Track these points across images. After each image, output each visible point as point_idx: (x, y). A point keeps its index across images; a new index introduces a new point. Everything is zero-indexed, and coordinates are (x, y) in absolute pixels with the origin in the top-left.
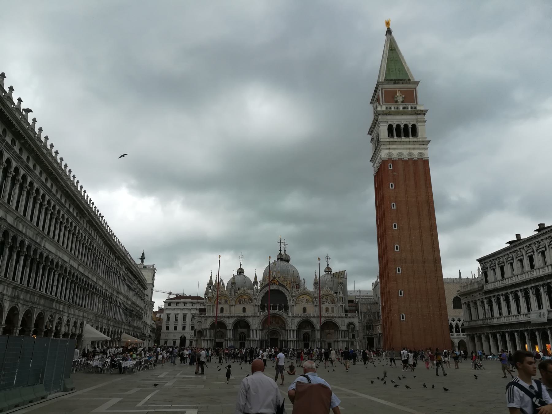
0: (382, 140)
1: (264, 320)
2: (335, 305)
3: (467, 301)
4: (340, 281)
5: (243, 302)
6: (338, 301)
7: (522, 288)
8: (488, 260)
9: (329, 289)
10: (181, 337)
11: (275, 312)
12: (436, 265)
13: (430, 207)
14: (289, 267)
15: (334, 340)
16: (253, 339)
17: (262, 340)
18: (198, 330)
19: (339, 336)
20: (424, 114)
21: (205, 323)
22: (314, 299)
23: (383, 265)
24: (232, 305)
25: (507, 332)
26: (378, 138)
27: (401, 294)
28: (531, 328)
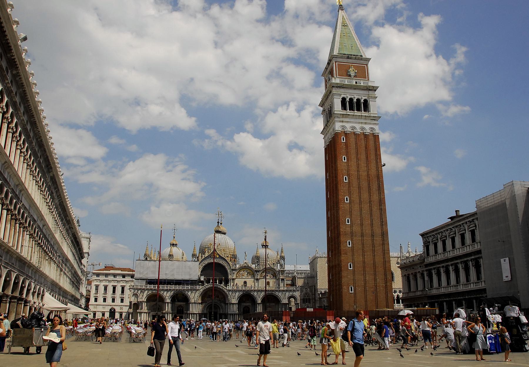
0: (335, 112)
2: (276, 279)
3: (406, 274)
7: (462, 260)
8: (431, 234)
10: (111, 310)
12: (384, 239)
13: (379, 182)
16: (192, 312)
20: (375, 90)
22: (255, 272)
23: (332, 238)
25: (445, 301)
26: (331, 111)
27: (350, 267)
28: (469, 297)
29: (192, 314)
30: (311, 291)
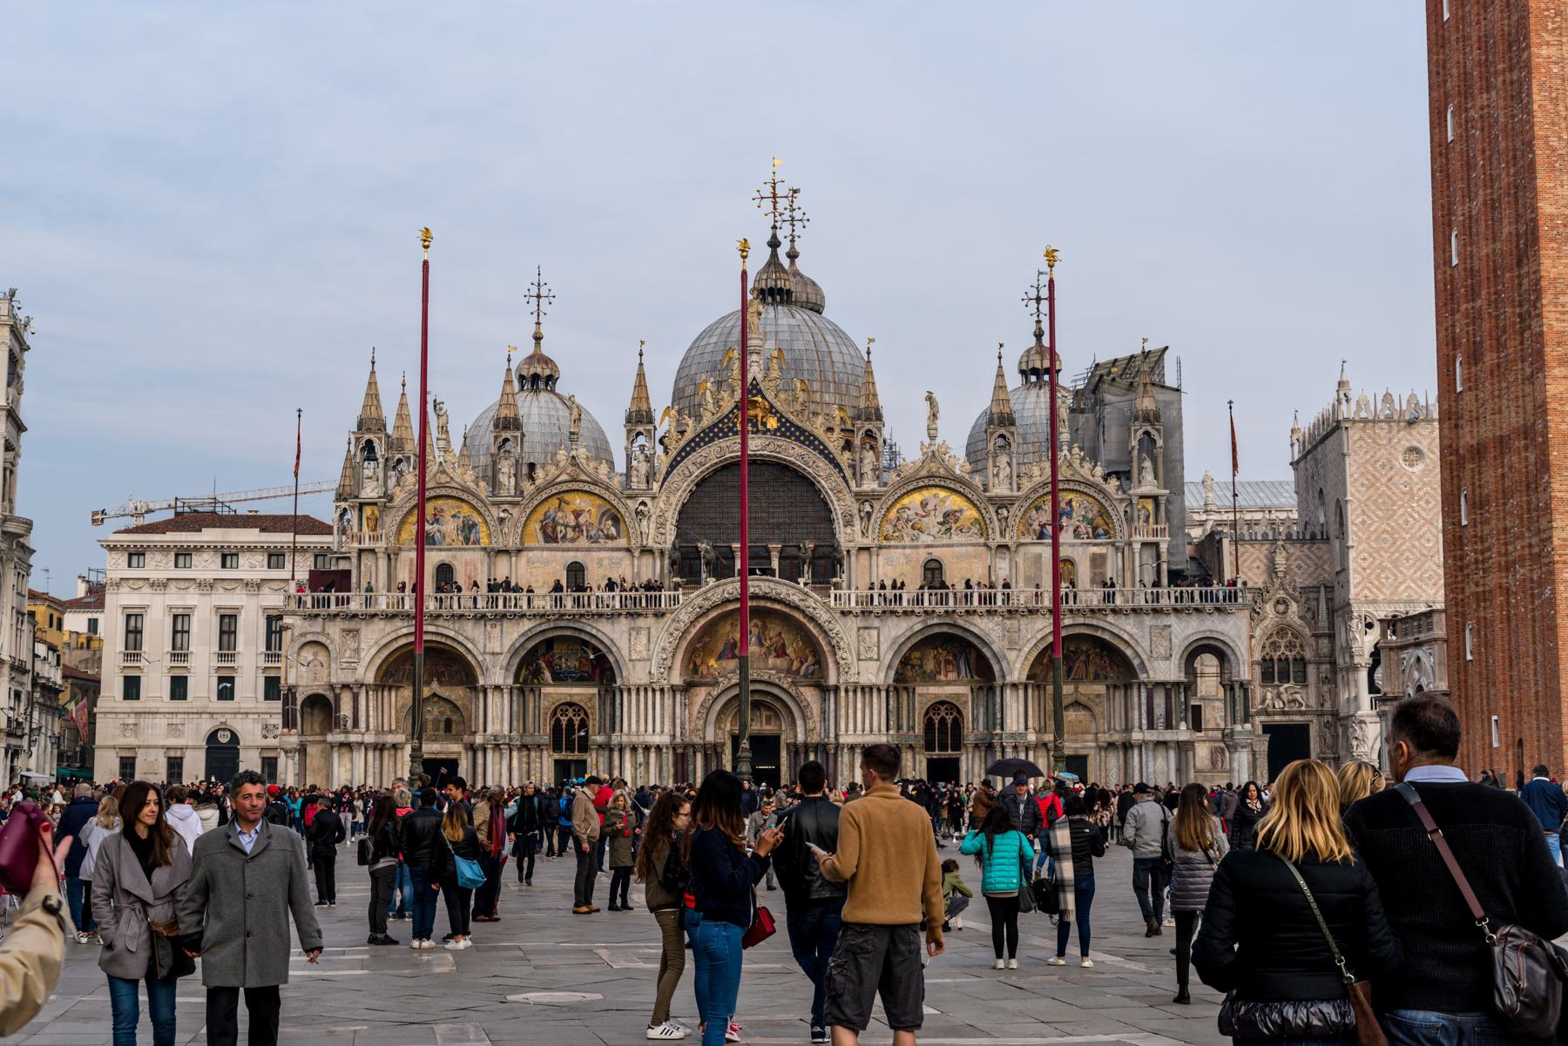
1: (694, 631)
2: (1113, 544)
4: (1147, 404)
5: (570, 534)
6: (1129, 519)
9: (1076, 450)
10: (213, 737)
11: (761, 584)
14: (830, 338)
15: (1104, 738)
16: (634, 739)
17: (686, 746)
18: (310, 692)
19: (1138, 716)
21: (348, 653)
23: (1471, 273)
24: (507, 552)
29: (634, 749)
30: (1309, 615)
